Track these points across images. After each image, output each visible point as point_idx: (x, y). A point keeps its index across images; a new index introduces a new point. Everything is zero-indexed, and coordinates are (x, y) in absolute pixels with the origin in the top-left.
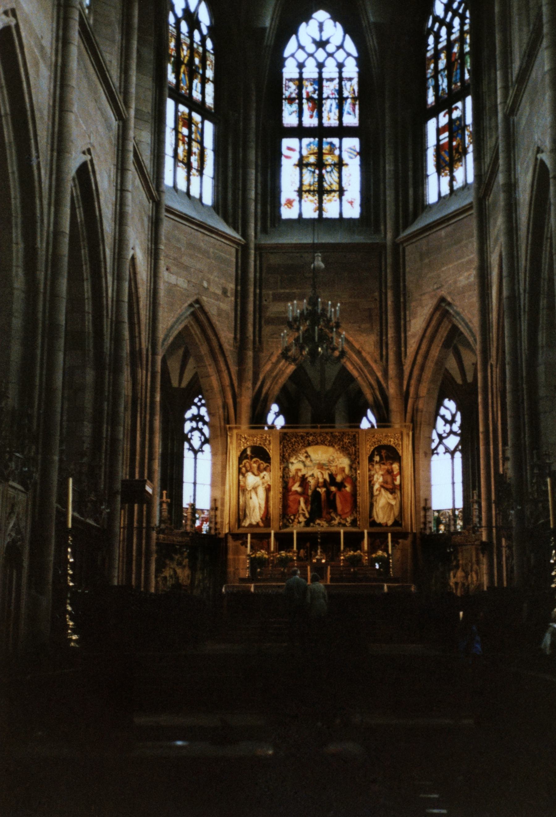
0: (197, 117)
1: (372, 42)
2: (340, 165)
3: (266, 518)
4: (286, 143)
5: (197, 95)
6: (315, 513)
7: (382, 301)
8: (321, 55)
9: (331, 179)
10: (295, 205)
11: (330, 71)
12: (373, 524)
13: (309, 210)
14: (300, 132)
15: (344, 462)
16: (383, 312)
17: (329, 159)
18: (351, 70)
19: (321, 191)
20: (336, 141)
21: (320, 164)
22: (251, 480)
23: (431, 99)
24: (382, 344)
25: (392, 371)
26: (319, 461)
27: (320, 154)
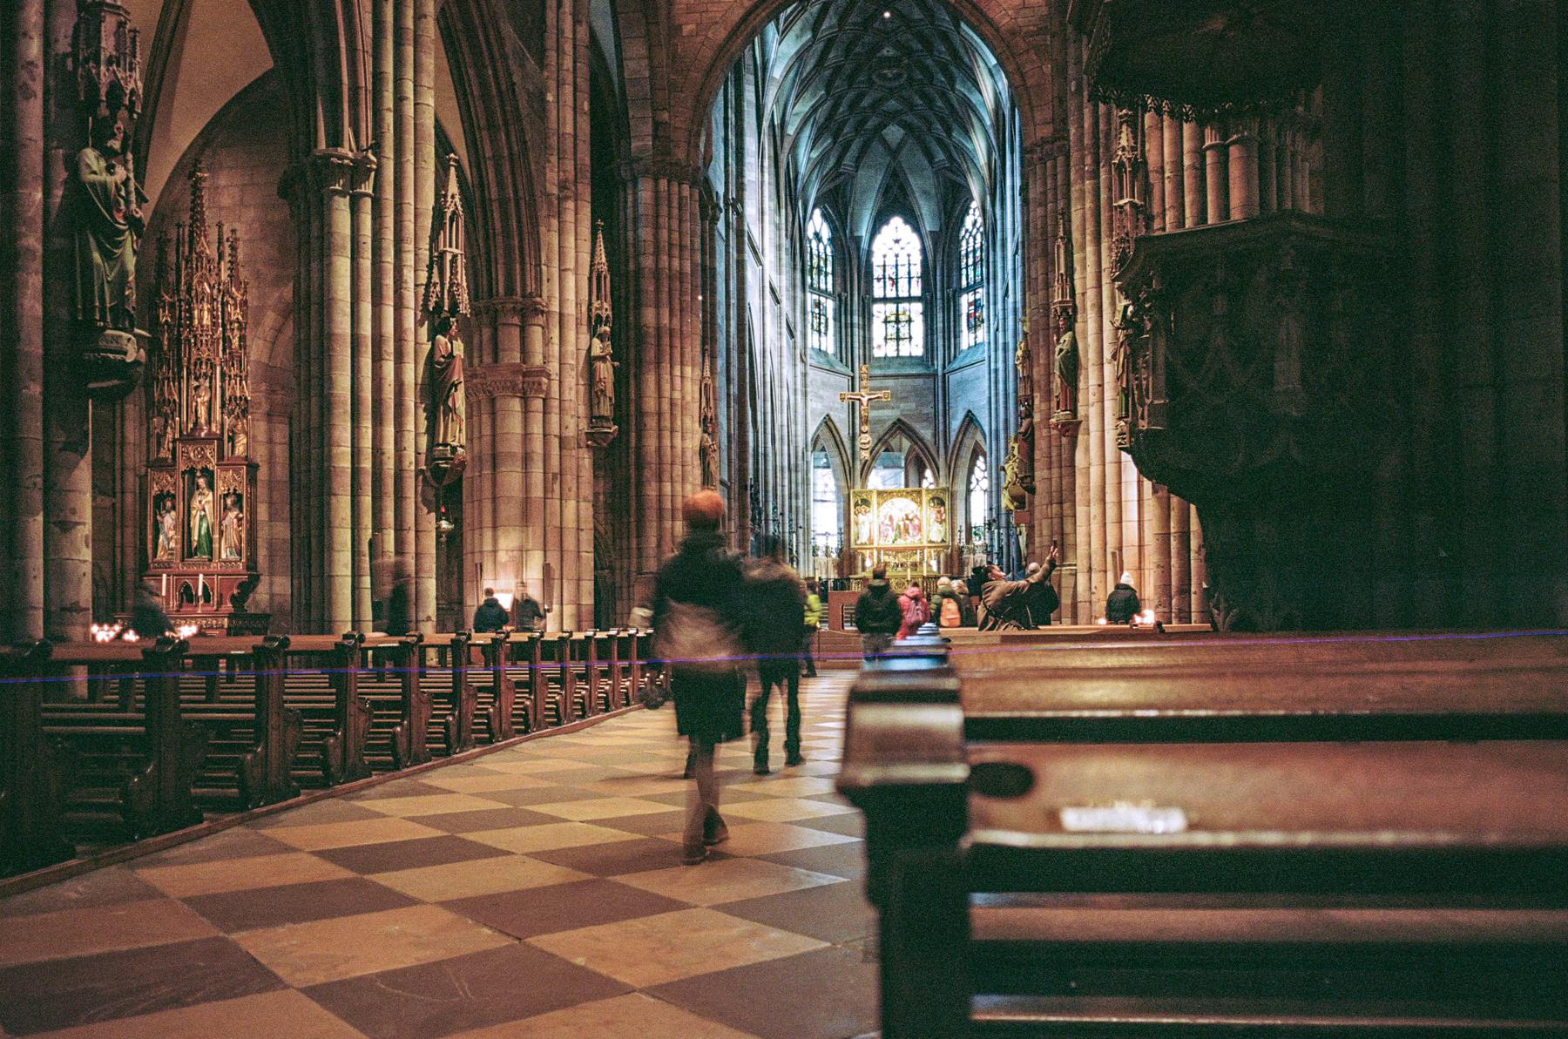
0: (823, 300)
1: (929, 243)
2: (910, 321)
4: (877, 309)
5: (823, 286)
7: (935, 407)
8: (897, 248)
9: (904, 331)
10: (882, 348)
11: (903, 260)
13: (892, 353)
14: (885, 300)
17: (902, 318)
18: (917, 258)
21: (897, 321)
24: (935, 435)
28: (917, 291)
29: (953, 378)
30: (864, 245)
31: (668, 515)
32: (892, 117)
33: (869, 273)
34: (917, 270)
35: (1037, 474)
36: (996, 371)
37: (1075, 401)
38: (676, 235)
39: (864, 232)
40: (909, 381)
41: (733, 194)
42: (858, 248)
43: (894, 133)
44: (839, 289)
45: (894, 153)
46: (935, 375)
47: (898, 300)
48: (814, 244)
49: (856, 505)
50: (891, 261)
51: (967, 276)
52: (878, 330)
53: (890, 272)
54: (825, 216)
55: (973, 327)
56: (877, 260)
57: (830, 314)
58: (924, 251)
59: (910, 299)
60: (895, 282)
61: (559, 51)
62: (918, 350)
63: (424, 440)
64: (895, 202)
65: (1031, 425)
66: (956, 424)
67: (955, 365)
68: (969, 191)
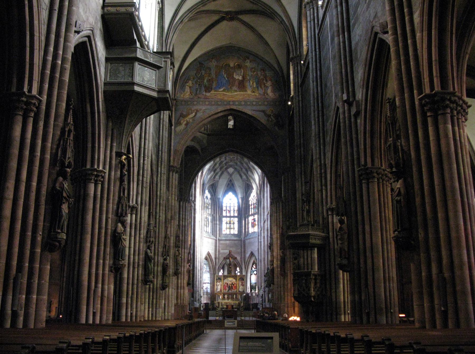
2: (234, 223)
3: (221, 290)
6: (229, 289)
9: (232, 226)
10: (225, 231)
11: (232, 205)
12: (239, 291)
13: (228, 232)
14: (226, 217)
15: (234, 280)
16: (241, 253)
17: (232, 222)
18: (236, 205)
19: (230, 228)
20: (233, 219)
21: (230, 223)
22: (218, 283)
23: (250, 213)
24: (241, 258)
25: (243, 264)
26: (230, 280)
27: (230, 221)
28: (236, 215)
29: (247, 242)
30: (221, 200)
31: (180, 288)
32: (231, 166)
33: (222, 209)
34: (236, 208)
35: (275, 280)
36: (261, 242)
37: (284, 269)
38: (184, 216)
39: (220, 196)
40: (233, 242)
41: (193, 199)
42: (219, 201)
43: (231, 170)
44: (212, 213)
45: (231, 175)
46: (241, 240)
47: (230, 217)
48: (206, 200)
49: (217, 280)
50: (228, 205)
51: (252, 211)
52: (224, 226)
53: (228, 208)
54: (209, 192)
55: (253, 226)
56: (224, 205)
57: (210, 221)
58: (238, 203)
59: (234, 217)
60: (230, 212)
61: (172, 188)
62: (236, 233)
63: (161, 282)
64: (230, 187)
65: (273, 267)
66: (248, 255)
67: (248, 238)
68: (252, 186)
